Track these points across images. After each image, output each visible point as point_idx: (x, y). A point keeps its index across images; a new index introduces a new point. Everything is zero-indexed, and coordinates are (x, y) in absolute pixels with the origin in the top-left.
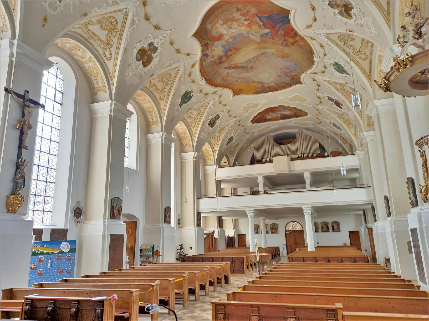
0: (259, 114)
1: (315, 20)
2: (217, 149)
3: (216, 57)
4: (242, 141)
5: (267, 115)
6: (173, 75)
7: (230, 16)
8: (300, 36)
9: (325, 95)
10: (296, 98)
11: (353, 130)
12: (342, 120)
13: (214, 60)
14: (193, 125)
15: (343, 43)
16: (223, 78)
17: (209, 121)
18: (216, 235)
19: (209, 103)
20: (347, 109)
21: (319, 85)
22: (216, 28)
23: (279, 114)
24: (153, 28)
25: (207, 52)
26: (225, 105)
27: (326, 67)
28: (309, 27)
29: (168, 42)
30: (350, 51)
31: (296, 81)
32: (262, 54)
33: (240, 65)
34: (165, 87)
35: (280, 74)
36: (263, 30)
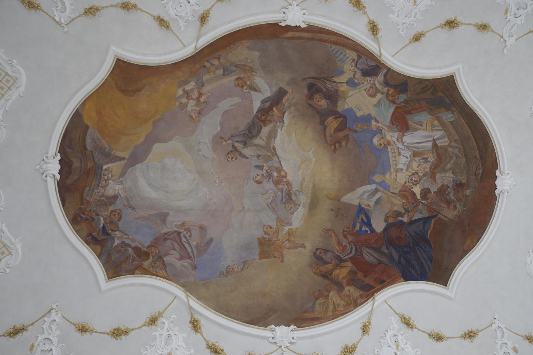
3: (344, 88)
7: (449, 166)
13: (336, 79)
22: (433, 126)
25: (380, 78)
36: (382, 218)
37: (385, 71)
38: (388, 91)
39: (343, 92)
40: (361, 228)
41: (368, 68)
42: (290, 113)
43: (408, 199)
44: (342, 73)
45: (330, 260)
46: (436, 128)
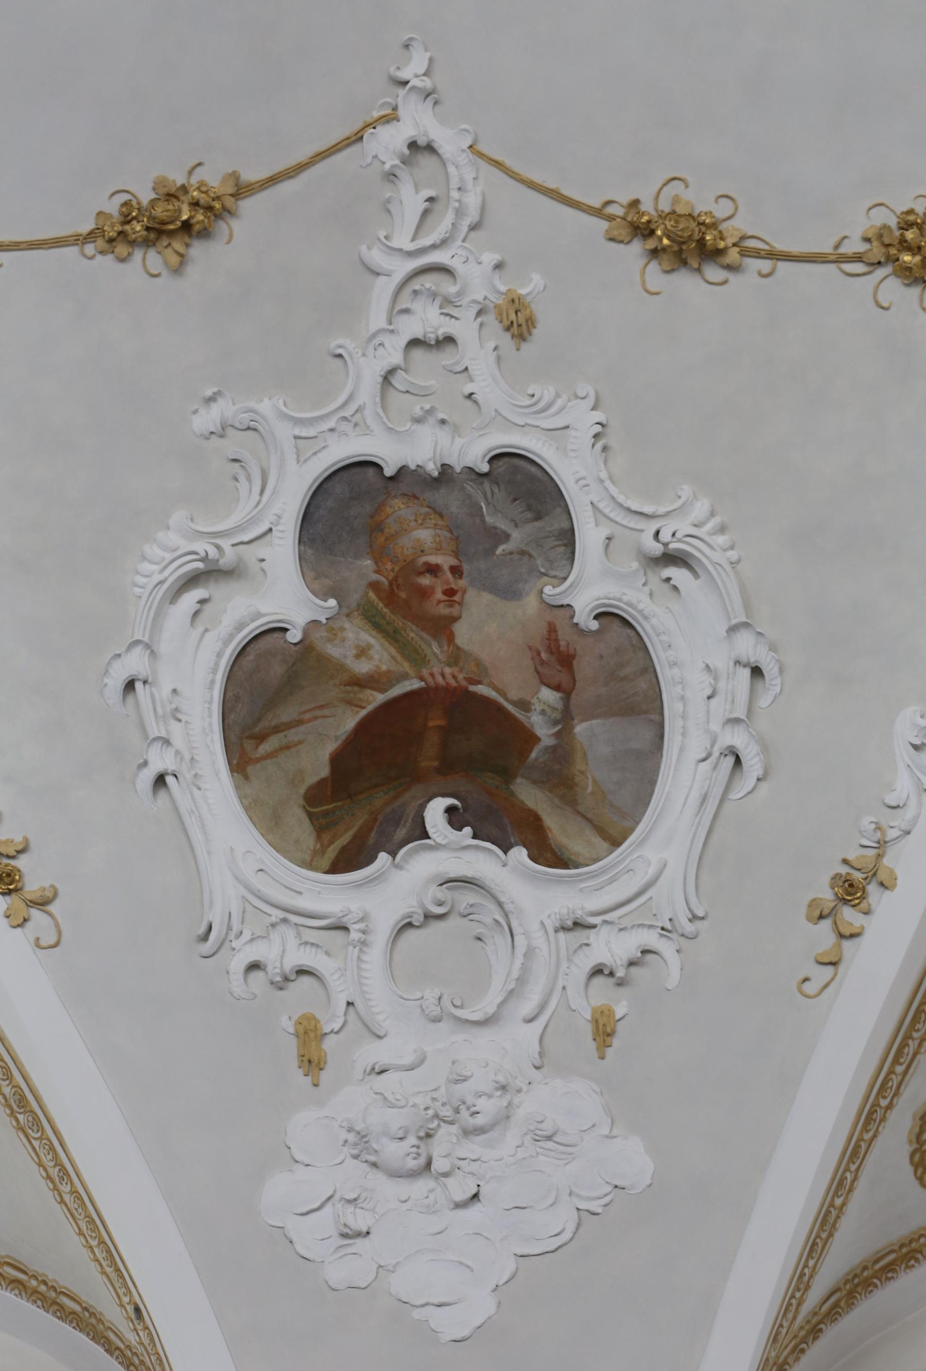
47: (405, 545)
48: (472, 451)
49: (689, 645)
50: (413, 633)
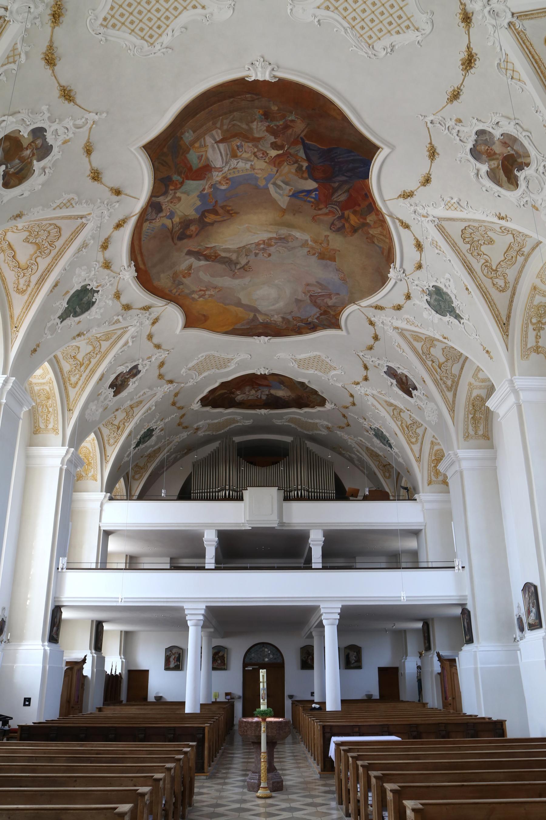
0: (223, 384)
1: (427, 181)
2: (113, 453)
3: (176, 220)
4: (169, 444)
5: (238, 392)
6: (66, 234)
7: (244, 126)
8: (378, 212)
9: (381, 362)
10: (316, 362)
11: (416, 448)
12: (399, 423)
13: (170, 226)
14: (73, 379)
15: (468, 246)
16: (175, 276)
17: (113, 377)
18: (87, 670)
19: (125, 332)
20: (424, 398)
21: (376, 338)
22: (201, 146)
23: (263, 394)
24: (56, 93)
26: (158, 347)
27: (408, 297)
28: (407, 195)
29: (83, 142)
30: (477, 266)
31: (329, 319)
32: (280, 239)
33: (223, 254)
34: (39, 260)
35: (301, 296)
36: (303, 182)
37: (154, 199)
38: (172, 190)
39: (180, 219)
40: (313, 198)
41: (154, 211)
42: (207, 244)
43: (284, 161)
44: (163, 225)
45: (341, 224)
46: (203, 143)
47: (483, 151)
48: (474, 137)
49: (510, 129)
50: (494, 157)
